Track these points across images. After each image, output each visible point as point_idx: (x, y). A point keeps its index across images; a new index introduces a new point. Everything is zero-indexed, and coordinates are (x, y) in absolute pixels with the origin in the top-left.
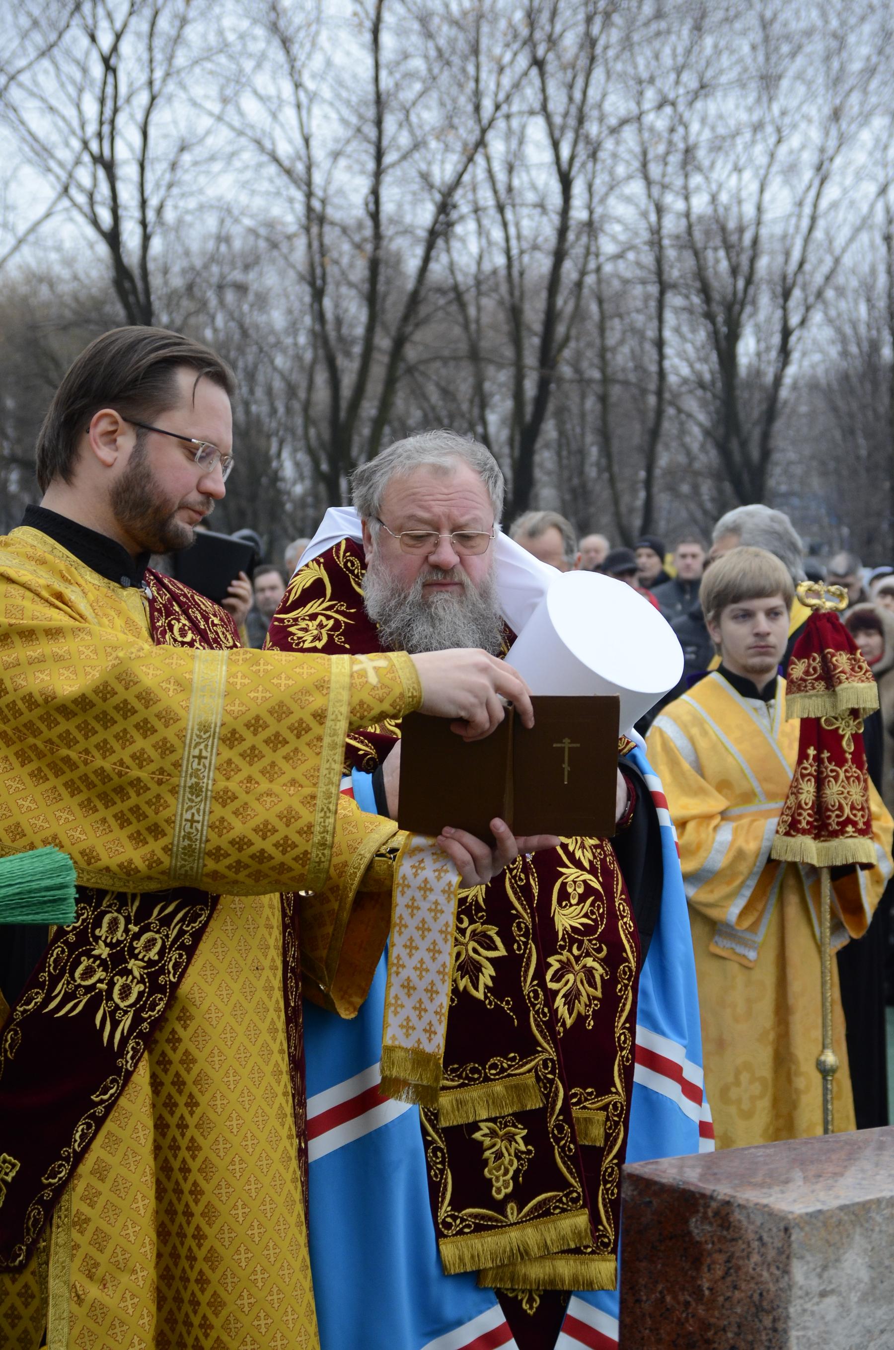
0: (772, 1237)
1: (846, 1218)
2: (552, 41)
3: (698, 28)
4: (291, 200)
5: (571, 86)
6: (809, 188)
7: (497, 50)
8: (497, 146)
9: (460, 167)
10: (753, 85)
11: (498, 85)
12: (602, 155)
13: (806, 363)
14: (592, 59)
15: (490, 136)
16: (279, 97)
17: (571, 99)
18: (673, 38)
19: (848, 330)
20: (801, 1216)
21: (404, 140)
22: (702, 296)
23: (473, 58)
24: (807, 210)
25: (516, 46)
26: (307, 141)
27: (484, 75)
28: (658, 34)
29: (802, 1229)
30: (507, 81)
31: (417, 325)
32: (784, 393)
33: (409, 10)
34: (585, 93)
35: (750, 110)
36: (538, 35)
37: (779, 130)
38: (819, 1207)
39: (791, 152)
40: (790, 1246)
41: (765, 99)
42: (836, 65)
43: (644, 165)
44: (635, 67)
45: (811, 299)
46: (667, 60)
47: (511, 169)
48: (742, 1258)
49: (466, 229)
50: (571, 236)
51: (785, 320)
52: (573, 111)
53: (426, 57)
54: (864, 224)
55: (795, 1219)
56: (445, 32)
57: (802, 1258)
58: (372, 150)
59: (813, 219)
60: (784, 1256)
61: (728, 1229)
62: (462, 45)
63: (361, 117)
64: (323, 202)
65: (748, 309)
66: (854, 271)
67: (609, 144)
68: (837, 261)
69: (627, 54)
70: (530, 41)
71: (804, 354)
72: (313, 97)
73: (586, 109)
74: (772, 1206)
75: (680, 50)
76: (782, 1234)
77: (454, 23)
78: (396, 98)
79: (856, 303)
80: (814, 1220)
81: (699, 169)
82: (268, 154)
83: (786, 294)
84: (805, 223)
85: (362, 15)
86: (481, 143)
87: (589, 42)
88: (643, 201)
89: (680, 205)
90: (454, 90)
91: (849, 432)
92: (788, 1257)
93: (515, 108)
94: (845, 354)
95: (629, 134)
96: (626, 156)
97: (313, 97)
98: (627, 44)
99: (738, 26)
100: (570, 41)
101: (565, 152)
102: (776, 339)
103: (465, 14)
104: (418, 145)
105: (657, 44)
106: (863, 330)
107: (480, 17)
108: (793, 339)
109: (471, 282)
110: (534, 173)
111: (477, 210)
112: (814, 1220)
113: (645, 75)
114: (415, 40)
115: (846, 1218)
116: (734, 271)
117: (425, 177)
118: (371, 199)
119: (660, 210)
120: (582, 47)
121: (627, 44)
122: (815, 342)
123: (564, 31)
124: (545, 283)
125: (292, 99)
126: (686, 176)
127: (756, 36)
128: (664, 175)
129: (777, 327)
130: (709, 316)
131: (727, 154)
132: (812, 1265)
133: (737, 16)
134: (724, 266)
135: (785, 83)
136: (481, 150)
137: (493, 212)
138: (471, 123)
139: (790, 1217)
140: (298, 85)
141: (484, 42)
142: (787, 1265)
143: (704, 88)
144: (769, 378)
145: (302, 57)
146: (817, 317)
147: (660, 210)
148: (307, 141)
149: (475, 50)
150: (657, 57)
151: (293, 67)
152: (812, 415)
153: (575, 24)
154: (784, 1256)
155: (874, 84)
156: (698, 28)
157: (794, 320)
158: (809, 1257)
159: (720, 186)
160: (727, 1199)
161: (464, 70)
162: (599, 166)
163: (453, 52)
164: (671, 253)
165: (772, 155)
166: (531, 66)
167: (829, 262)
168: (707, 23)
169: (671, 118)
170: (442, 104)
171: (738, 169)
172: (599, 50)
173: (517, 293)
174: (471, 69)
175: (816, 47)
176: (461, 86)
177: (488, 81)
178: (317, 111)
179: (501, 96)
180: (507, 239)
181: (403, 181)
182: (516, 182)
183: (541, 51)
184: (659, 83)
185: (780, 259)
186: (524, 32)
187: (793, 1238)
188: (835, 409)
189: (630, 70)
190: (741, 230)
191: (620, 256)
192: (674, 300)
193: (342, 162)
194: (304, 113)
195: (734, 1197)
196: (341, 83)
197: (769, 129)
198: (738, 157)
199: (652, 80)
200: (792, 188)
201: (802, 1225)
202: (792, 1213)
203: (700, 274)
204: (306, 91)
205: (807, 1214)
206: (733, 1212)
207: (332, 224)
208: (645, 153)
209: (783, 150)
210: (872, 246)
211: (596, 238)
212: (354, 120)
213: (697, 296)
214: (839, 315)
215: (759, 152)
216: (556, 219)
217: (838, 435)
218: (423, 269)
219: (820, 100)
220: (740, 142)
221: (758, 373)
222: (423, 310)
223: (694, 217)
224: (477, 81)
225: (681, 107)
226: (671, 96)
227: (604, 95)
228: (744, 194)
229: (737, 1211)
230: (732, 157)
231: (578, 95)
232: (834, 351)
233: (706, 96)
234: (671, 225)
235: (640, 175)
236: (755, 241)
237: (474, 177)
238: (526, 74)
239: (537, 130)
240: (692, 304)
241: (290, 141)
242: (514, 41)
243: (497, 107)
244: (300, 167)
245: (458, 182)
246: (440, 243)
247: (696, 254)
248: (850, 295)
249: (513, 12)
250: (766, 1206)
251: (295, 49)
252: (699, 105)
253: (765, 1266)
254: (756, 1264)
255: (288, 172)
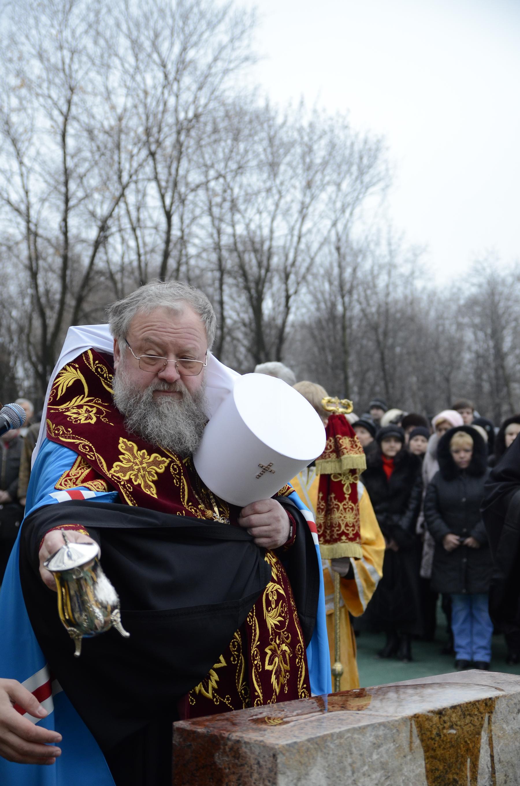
0: (265, 761)
1: (312, 746)
2: (159, 143)
3: (236, 139)
4: (18, 224)
5: (169, 167)
6: (296, 221)
7: (130, 147)
8: (131, 198)
9: (110, 209)
10: (266, 169)
11: (131, 166)
12: (187, 202)
13: (298, 313)
14: (181, 153)
15: (127, 192)
16: (10, 170)
17: (170, 174)
18: (223, 144)
19: (319, 296)
20: (283, 746)
21: (80, 194)
22: (243, 277)
23: (116, 152)
24: (296, 233)
25: (140, 145)
26: (27, 192)
27: (123, 161)
28: (215, 141)
29: (284, 754)
30: (135, 165)
31: (90, 290)
32: (288, 329)
33: (81, 126)
34: (177, 170)
35: (265, 182)
36: (152, 139)
37: (280, 192)
38: (295, 740)
39: (286, 203)
40: (276, 766)
41: (272, 176)
42: (308, 160)
43: (210, 209)
44: (203, 158)
45: (300, 279)
46: (221, 155)
47: (138, 209)
48: (247, 777)
49: (115, 241)
50: (171, 245)
51: (287, 290)
52: (172, 179)
53: (92, 152)
54: (326, 241)
55: (279, 748)
56: (101, 137)
57: (284, 773)
58: (63, 198)
59: (300, 238)
60: (273, 773)
61: (238, 758)
62: (110, 145)
63: (57, 181)
64: (36, 225)
65: (267, 285)
66: (321, 265)
67: (190, 197)
68: (312, 259)
69: (198, 152)
70: (147, 143)
71: (298, 308)
72: (30, 170)
73: (179, 178)
74: (265, 741)
75: (227, 151)
76: (272, 759)
77: (106, 132)
78: (75, 171)
79: (323, 283)
80: (291, 749)
81: (239, 211)
82: (5, 200)
83: (287, 277)
84: (295, 239)
85: (55, 126)
86: (123, 195)
87: (179, 145)
88: (210, 229)
89: (229, 230)
90: (108, 168)
91: (322, 349)
92: (276, 774)
93: (141, 176)
94: (318, 309)
95: (201, 193)
96: (201, 204)
97: (30, 170)
98: (199, 146)
99: (256, 138)
100: (169, 142)
101: (168, 201)
102: (283, 300)
103: (112, 128)
104: (87, 196)
105: (215, 146)
106: (327, 296)
107: (120, 131)
108: (291, 300)
109: (118, 268)
110: (151, 211)
111: (120, 230)
112: (291, 749)
113: (209, 163)
114: (85, 140)
115: (312, 746)
116: (260, 265)
117: (93, 214)
118: (63, 224)
119: (219, 232)
120: (174, 147)
121: (199, 146)
122: (302, 302)
123: (166, 137)
124: (158, 270)
125: (18, 171)
126: (233, 215)
127: (266, 143)
128: (221, 213)
129: (283, 294)
130: (247, 288)
131: (253, 205)
132: (291, 778)
133: (256, 133)
134: (254, 262)
135: (282, 168)
136: (122, 199)
137: (129, 231)
138: (117, 185)
139: (277, 747)
140: (21, 163)
141: (123, 144)
142: (275, 779)
143: (240, 169)
144: (279, 321)
145: (23, 149)
146: (303, 290)
147: (219, 232)
148: (27, 192)
149: (118, 147)
150: (215, 152)
151: (18, 154)
152: (303, 341)
153: (170, 135)
154: (273, 773)
155: (328, 170)
156: (236, 139)
157: (291, 291)
158: (289, 773)
159: (251, 220)
160: (238, 739)
161: (112, 158)
162: (186, 208)
163: (106, 147)
164: (225, 254)
165: (277, 205)
166: (147, 156)
167: (308, 260)
168: (241, 137)
169: (223, 185)
170: (101, 175)
171: (260, 212)
172: (183, 149)
173: (143, 276)
174: (116, 158)
175: (298, 150)
176: (111, 166)
177: (126, 166)
178: (32, 177)
179: (133, 171)
180: (138, 246)
181: (80, 215)
182: (142, 216)
183: (153, 147)
184: (216, 166)
185: (283, 259)
186: (144, 138)
187: (278, 761)
188: (314, 337)
189: (201, 160)
190: (262, 243)
191: (198, 256)
192: (228, 280)
193: (47, 204)
194: (25, 178)
195: (242, 737)
196: (44, 162)
197: (274, 191)
198: (259, 204)
199: (212, 166)
200: (288, 222)
201: (284, 752)
202: (277, 744)
203: (242, 266)
204: (25, 166)
205: (287, 745)
206: (241, 747)
207: (41, 237)
208: (210, 202)
209: (282, 202)
210: (330, 252)
211: (186, 248)
212: (52, 182)
213: (241, 277)
214: (315, 288)
215: (270, 204)
216: (164, 236)
217: (316, 350)
218: (92, 263)
219: (300, 178)
220: (260, 200)
221: (274, 319)
222: (92, 283)
223: (237, 237)
224: (119, 163)
225: (229, 178)
226: (223, 172)
227: (188, 171)
228: (263, 224)
229: (244, 746)
230: (256, 205)
231: (173, 171)
232: (313, 307)
233: (242, 173)
234: (225, 240)
235: (208, 213)
236: (270, 248)
237: (119, 213)
238: (145, 160)
239: (152, 189)
240: (238, 282)
241: (17, 192)
242: (139, 142)
243: (131, 177)
244: (23, 207)
245: (110, 215)
246: (101, 249)
247: (239, 257)
248: (320, 278)
249: (137, 127)
250: (261, 741)
251: (19, 145)
252: (238, 179)
253: (261, 781)
254: (256, 780)
255: (17, 210)
